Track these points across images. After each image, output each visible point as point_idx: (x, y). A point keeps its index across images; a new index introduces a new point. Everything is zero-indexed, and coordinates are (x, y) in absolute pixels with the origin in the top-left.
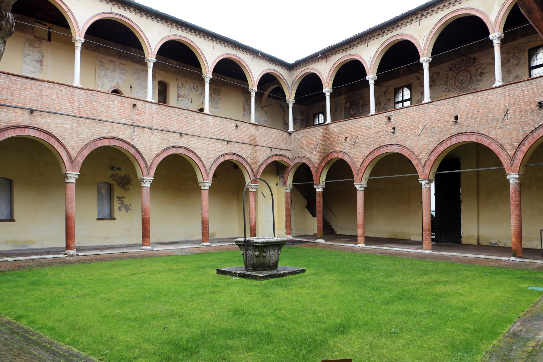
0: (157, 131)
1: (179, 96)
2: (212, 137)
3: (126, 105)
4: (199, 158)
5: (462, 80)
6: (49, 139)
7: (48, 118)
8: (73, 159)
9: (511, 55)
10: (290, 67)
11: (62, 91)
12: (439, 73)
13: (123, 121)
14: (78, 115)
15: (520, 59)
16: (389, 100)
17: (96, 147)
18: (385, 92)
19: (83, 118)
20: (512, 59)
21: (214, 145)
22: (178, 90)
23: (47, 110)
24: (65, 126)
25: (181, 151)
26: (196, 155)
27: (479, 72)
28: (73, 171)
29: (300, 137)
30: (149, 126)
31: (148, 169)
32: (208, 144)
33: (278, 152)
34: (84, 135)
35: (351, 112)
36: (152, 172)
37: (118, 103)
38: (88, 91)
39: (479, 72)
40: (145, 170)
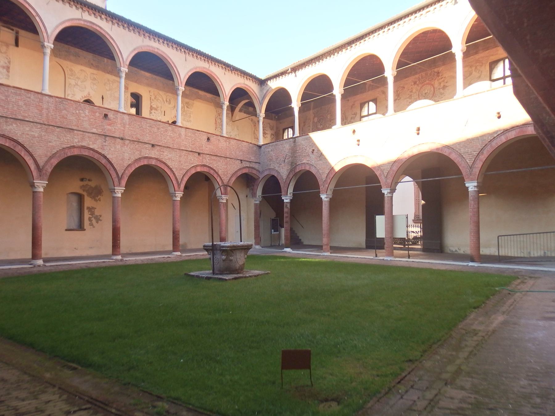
0: (128, 141)
1: (151, 108)
2: (184, 149)
3: (97, 114)
4: (171, 169)
5: (425, 94)
6: (15, 147)
7: (14, 125)
8: (41, 167)
9: (473, 68)
10: (262, 83)
11: (30, 98)
12: (404, 87)
13: (94, 130)
14: (46, 123)
15: (482, 72)
16: (355, 114)
17: (66, 156)
18: (352, 107)
19: (52, 126)
20: (474, 73)
21: (186, 157)
22: (151, 103)
23: (14, 117)
24: (33, 133)
25: (153, 162)
26: (168, 167)
27: (442, 85)
28: (41, 180)
29: (270, 150)
30: (121, 136)
31: (120, 179)
32: (180, 156)
33: (248, 165)
34: (54, 144)
35: (319, 126)
36: (124, 182)
37: (89, 112)
38: (57, 99)
39: (442, 85)
40: (116, 180)
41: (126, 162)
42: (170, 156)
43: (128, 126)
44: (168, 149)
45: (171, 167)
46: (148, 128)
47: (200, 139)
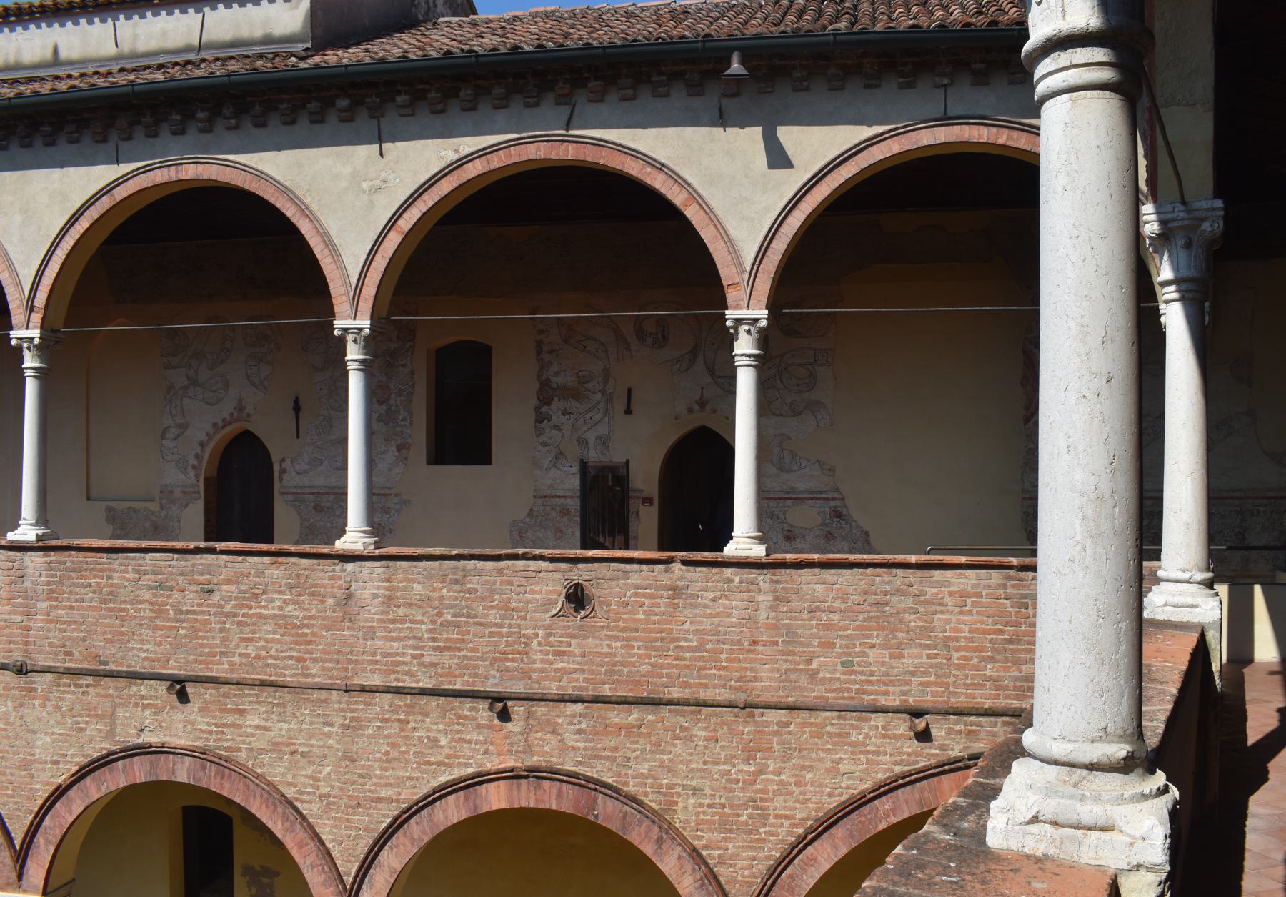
0: (49, 677)
1: (546, 394)
2: (377, 680)
21: (392, 729)
30: (17, 656)
32: (352, 727)
41: (45, 776)
42: (281, 729)
43: (43, 605)
44: (268, 695)
45: (290, 793)
46: (147, 595)
47: (505, 605)
